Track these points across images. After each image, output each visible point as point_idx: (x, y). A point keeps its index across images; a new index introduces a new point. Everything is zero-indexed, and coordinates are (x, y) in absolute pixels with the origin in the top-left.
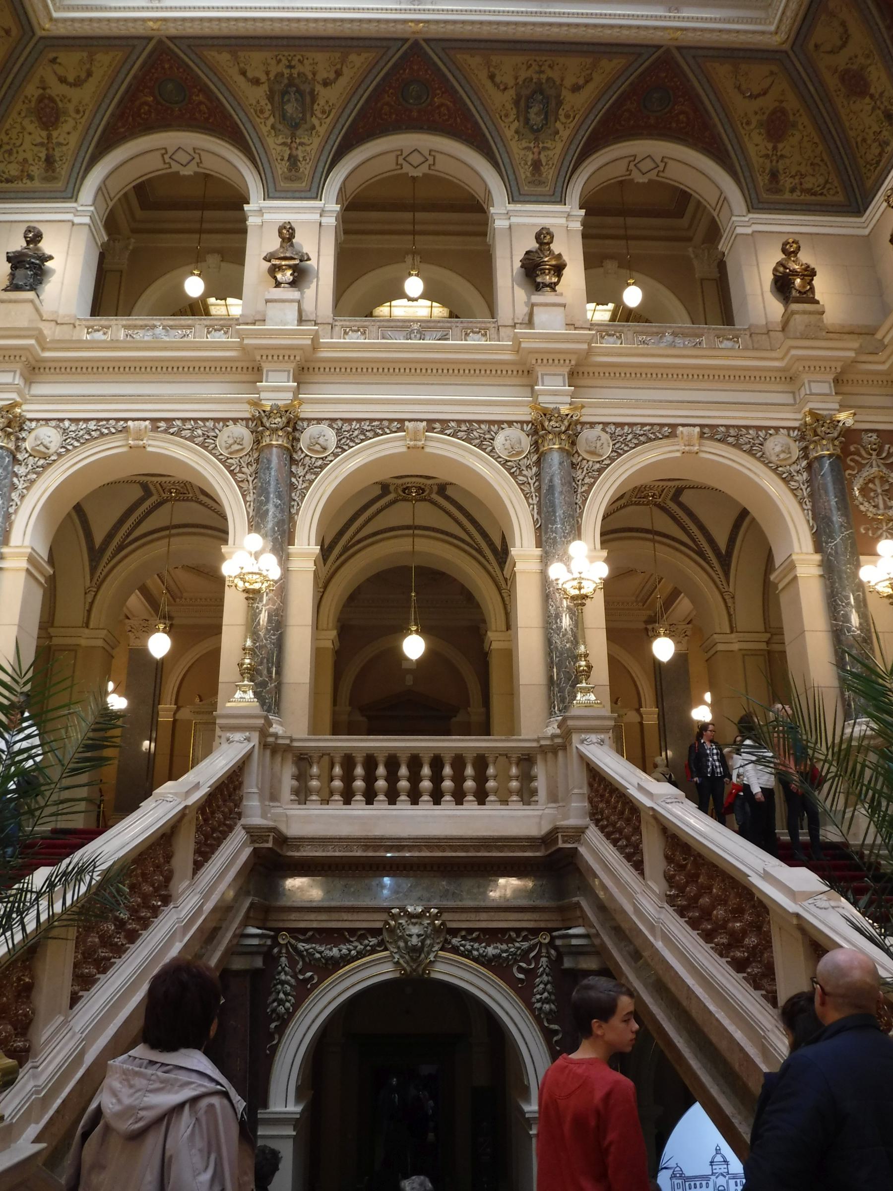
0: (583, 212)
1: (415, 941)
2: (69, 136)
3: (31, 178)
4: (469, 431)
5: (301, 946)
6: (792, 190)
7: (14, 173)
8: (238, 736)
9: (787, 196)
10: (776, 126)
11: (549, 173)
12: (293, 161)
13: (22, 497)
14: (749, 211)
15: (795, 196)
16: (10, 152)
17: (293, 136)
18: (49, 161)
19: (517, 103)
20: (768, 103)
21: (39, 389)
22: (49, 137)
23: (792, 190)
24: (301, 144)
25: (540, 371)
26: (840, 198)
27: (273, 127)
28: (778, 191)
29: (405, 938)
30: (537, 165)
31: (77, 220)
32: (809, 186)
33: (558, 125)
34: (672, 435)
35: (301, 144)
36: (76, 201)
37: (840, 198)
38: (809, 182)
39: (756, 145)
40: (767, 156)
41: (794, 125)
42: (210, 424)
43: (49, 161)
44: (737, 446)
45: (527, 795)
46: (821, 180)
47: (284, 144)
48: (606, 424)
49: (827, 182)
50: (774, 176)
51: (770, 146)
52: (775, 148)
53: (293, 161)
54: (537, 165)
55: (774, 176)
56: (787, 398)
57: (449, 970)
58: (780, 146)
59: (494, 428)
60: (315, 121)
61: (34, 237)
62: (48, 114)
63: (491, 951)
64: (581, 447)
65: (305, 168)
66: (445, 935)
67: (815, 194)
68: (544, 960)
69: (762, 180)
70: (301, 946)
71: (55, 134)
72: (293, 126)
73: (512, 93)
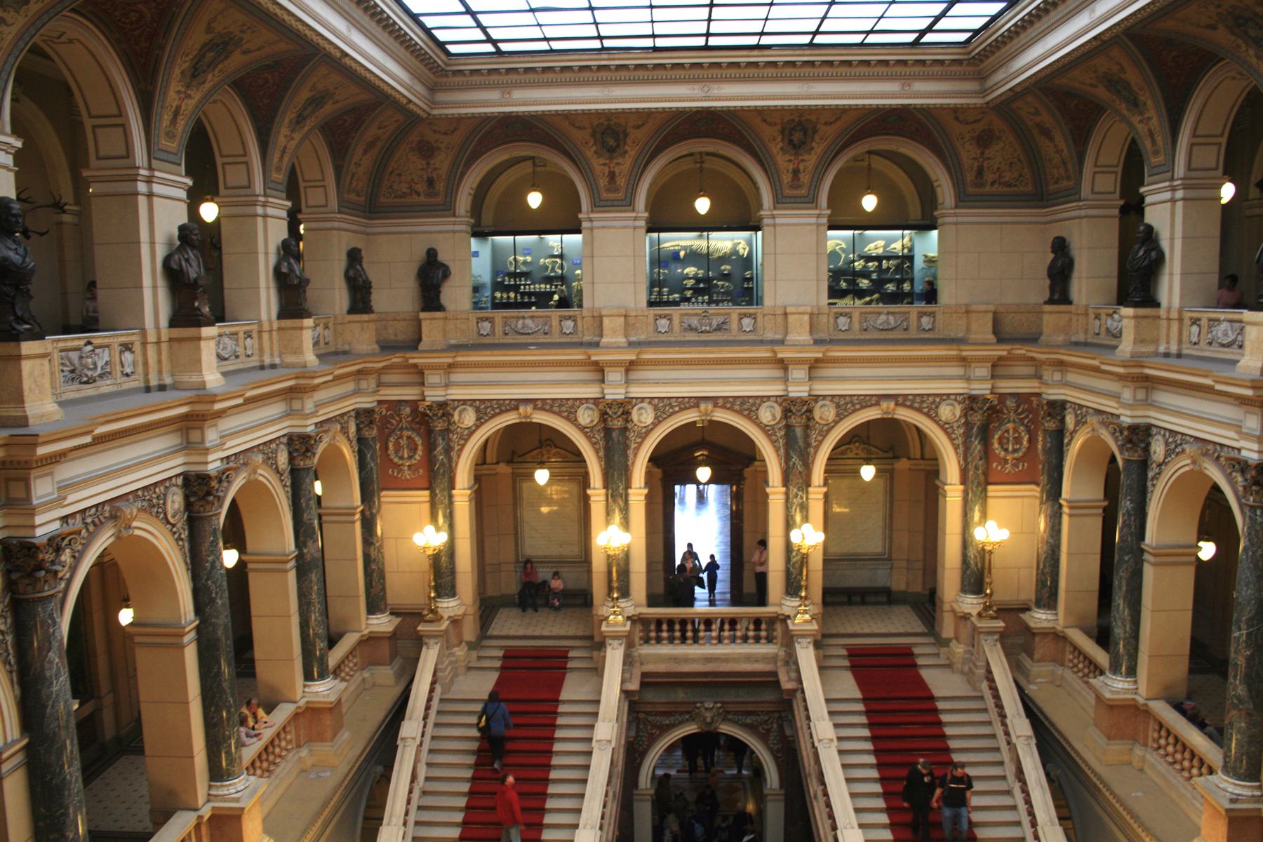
0: (829, 212)
1: (709, 720)
2: (442, 162)
3: (419, 195)
4: (742, 404)
5: (650, 718)
6: (993, 184)
7: (404, 190)
8: (616, 643)
9: (988, 189)
10: (985, 140)
11: (805, 178)
12: (612, 176)
13: (459, 456)
14: (956, 207)
15: (994, 189)
16: (400, 175)
17: (611, 159)
18: (431, 182)
19: (782, 132)
20: (980, 127)
21: (455, 377)
22: (428, 164)
23: (993, 184)
24: (618, 164)
25: (791, 367)
26: (1030, 188)
27: (595, 152)
28: (982, 185)
29: (705, 718)
30: (796, 172)
31: (457, 228)
32: (1006, 179)
33: (814, 144)
34: (877, 404)
35: (618, 164)
36: (454, 216)
37: (1030, 188)
38: (1008, 177)
39: (968, 153)
40: (975, 159)
41: (999, 138)
42: (570, 403)
43: (431, 182)
44: (919, 410)
45: (770, 640)
46: (1016, 175)
47: (605, 164)
48: (833, 396)
49: (1021, 175)
50: (980, 172)
51: (979, 152)
52: (982, 153)
53: (612, 176)
54: (796, 172)
55: (980, 172)
56: (959, 371)
57: (725, 728)
58: (987, 151)
59: (758, 401)
60: (627, 148)
61: (432, 254)
62: (426, 150)
63: (748, 721)
64: (817, 414)
65: (621, 182)
66: (726, 716)
67: (1010, 186)
68: (775, 726)
69: (970, 177)
70: (650, 718)
71: (432, 162)
72: (611, 151)
73: (779, 127)
